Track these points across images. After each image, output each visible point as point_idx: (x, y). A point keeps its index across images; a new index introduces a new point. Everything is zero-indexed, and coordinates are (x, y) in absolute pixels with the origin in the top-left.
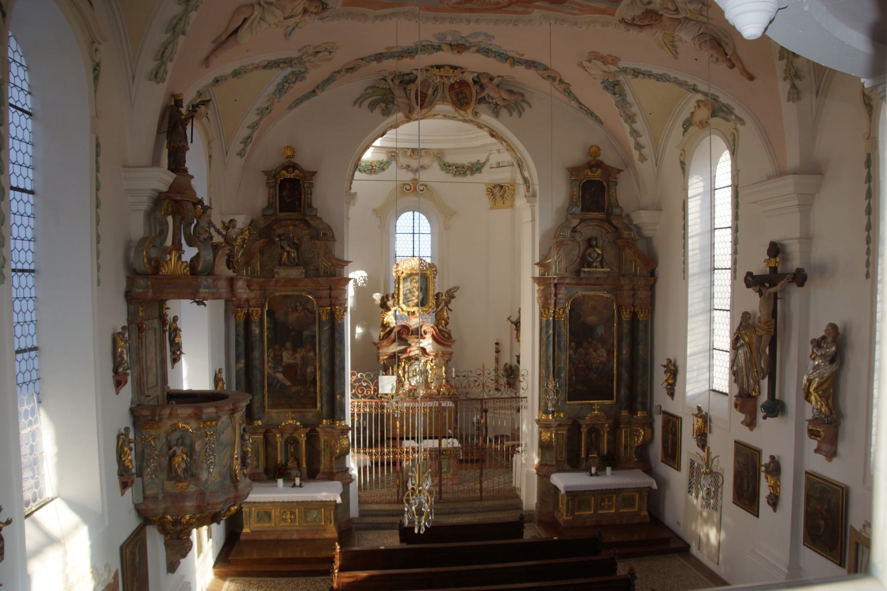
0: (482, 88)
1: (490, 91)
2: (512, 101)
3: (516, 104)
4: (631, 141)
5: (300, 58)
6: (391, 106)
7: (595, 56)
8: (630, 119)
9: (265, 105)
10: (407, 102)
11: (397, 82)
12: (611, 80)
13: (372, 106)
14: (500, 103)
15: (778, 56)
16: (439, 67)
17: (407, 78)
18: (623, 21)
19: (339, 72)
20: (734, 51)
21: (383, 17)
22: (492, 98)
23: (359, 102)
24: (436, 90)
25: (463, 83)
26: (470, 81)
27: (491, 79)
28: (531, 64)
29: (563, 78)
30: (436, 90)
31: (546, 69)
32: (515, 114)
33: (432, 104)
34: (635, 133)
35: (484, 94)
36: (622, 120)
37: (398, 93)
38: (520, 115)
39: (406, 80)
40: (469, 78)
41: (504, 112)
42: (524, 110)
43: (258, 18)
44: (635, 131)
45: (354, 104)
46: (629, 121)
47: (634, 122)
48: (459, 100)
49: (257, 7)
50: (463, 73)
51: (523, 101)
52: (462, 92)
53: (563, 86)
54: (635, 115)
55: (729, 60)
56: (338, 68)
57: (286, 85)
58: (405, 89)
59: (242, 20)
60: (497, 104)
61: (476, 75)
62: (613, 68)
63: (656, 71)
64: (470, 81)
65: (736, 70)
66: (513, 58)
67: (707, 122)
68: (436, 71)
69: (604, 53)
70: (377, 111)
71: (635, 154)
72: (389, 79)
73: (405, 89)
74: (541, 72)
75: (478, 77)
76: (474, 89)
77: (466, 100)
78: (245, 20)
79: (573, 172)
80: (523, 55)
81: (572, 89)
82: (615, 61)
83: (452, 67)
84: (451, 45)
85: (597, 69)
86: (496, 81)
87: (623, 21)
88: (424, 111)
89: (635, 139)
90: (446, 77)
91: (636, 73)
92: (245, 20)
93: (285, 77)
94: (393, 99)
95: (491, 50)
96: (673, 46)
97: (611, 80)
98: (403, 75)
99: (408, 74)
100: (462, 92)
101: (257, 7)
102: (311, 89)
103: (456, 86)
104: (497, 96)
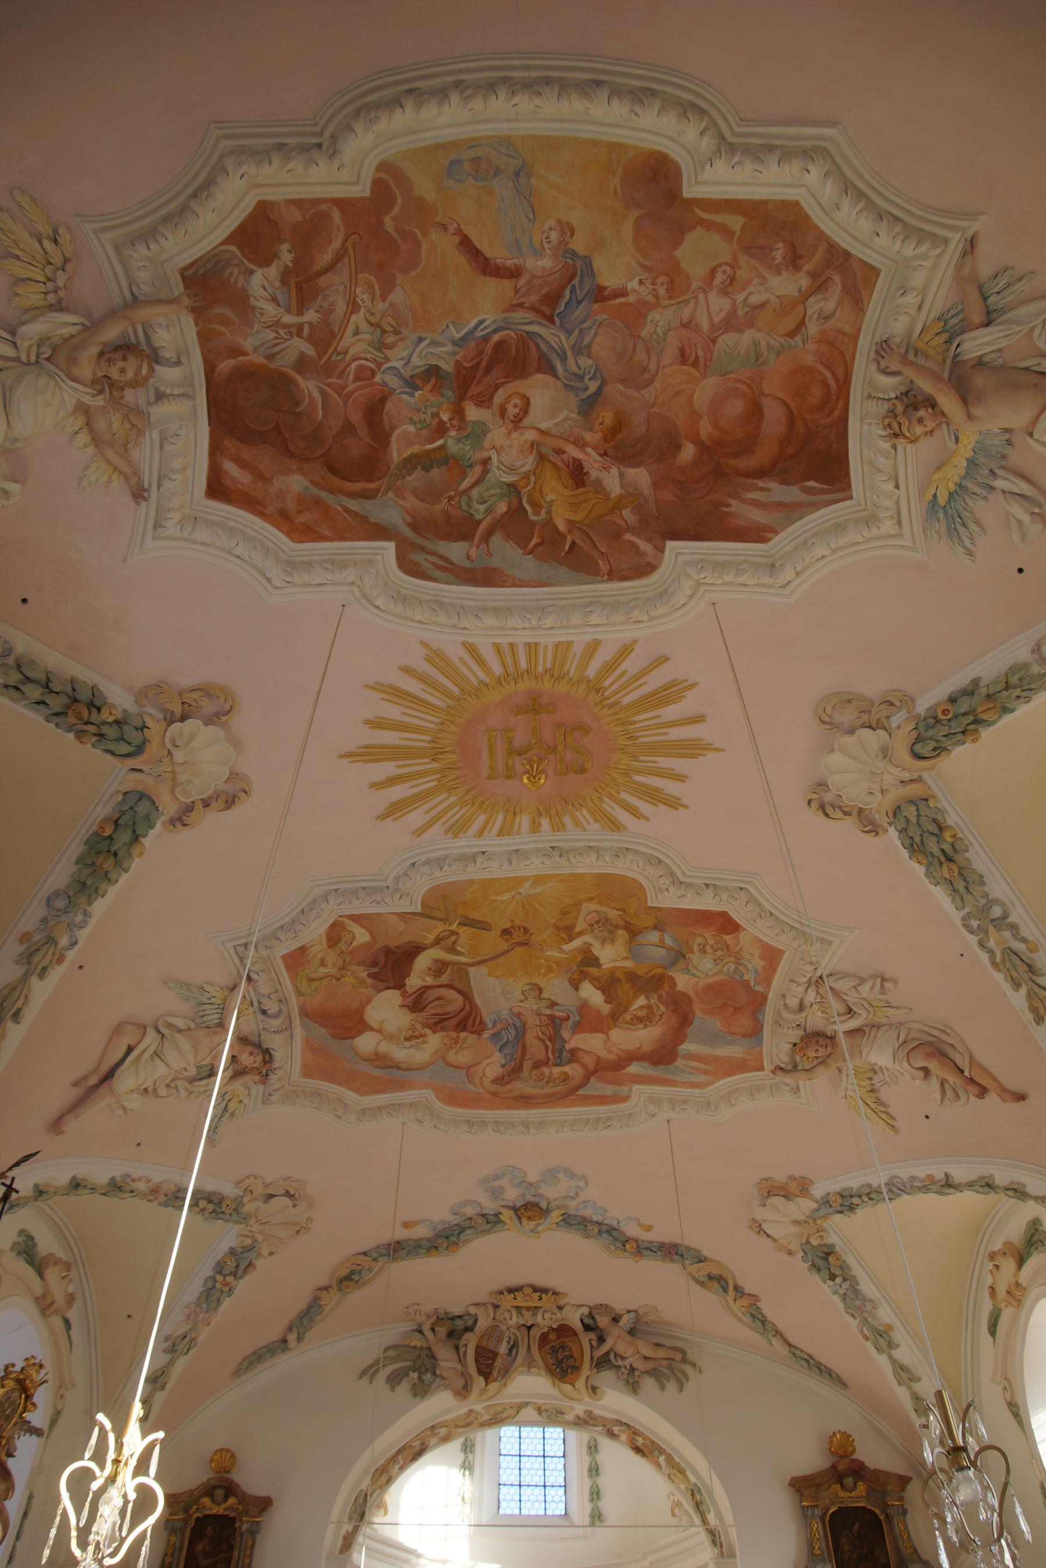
0: (601, 1340)
1: (616, 1341)
2: (660, 1359)
3: (670, 1367)
4: (902, 1394)
5: (239, 1203)
6: (428, 1377)
7: (773, 1190)
8: (883, 1338)
9: (181, 1331)
10: (459, 1367)
11: (442, 1331)
12: (815, 1242)
13: (394, 1380)
14: (640, 1365)
15: (1031, 1017)
16: (511, 1290)
17: (459, 1324)
18: (779, 1069)
19: (326, 1288)
20: (972, 1060)
21: (375, 1112)
22: (623, 1358)
23: (369, 1372)
24: (514, 1346)
25: (564, 1330)
26: (578, 1326)
27: (616, 1320)
28: (670, 1251)
29: (740, 1283)
30: (514, 1346)
31: (701, 1260)
32: (671, 1386)
33: (506, 1372)
34: (900, 1369)
35: (605, 1348)
36: (869, 1345)
37: (445, 1355)
38: (681, 1388)
39: (454, 1328)
40: (574, 1319)
41: (649, 1384)
42: (687, 1379)
43: (151, 1051)
44: (902, 1368)
45: (361, 1377)
46: (882, 1343)
47: (891, 1345)
48: (559, 1363)
49: (151, 1031)
50: (560, 1308)
51: (684, 1360)
52: (563, 1347)
53: (744, 1302)
54: (889, 1327)
55: (971, 1081)
56: (324, 1281)
57: (220, 1278)
58: (457, 1348)
59: (123, 1050)
60: (633, 1369)
61: (585, 1311)
62: (805, 1206)
63: (878, 1178)
64: (578, 1326)
65: (992, 1098)
66: (636, 1241)
67: (1018, 1285)
68: (508, 1301)
69: (780, 1176)
70: (404, 1387)
72: (426, 1328)
73: (457, 1348)
74: (693, 1269)
75: (591, 1315)
76: (586, 1339)
77: (571, 1362)
78: (130, 1049)
79: (803, 1487)
80: (649, 1228)
81: (767, 1307)
82: (802, 1187)
83: (535, 1289)
84: (515, 1209)
85: (783, 1219)
86: (626, 1321)
87: (779, 1069)
88: (493, 1386)
89: (910, 1388)
90: (528, 1309)
91: (847, 1202)
92: (130, 1049)
93: (218, 1263)
94: (434, 1366)
95: (591, 1221)
96: (879, 1101)
97: (815, 1242)
98: (452, 1319)
99: (460, 1317)
100: (563, 1347)
101: (151, 1031)
102: (274, 1333)
103: (553, 1336)
104: (630, 1352)
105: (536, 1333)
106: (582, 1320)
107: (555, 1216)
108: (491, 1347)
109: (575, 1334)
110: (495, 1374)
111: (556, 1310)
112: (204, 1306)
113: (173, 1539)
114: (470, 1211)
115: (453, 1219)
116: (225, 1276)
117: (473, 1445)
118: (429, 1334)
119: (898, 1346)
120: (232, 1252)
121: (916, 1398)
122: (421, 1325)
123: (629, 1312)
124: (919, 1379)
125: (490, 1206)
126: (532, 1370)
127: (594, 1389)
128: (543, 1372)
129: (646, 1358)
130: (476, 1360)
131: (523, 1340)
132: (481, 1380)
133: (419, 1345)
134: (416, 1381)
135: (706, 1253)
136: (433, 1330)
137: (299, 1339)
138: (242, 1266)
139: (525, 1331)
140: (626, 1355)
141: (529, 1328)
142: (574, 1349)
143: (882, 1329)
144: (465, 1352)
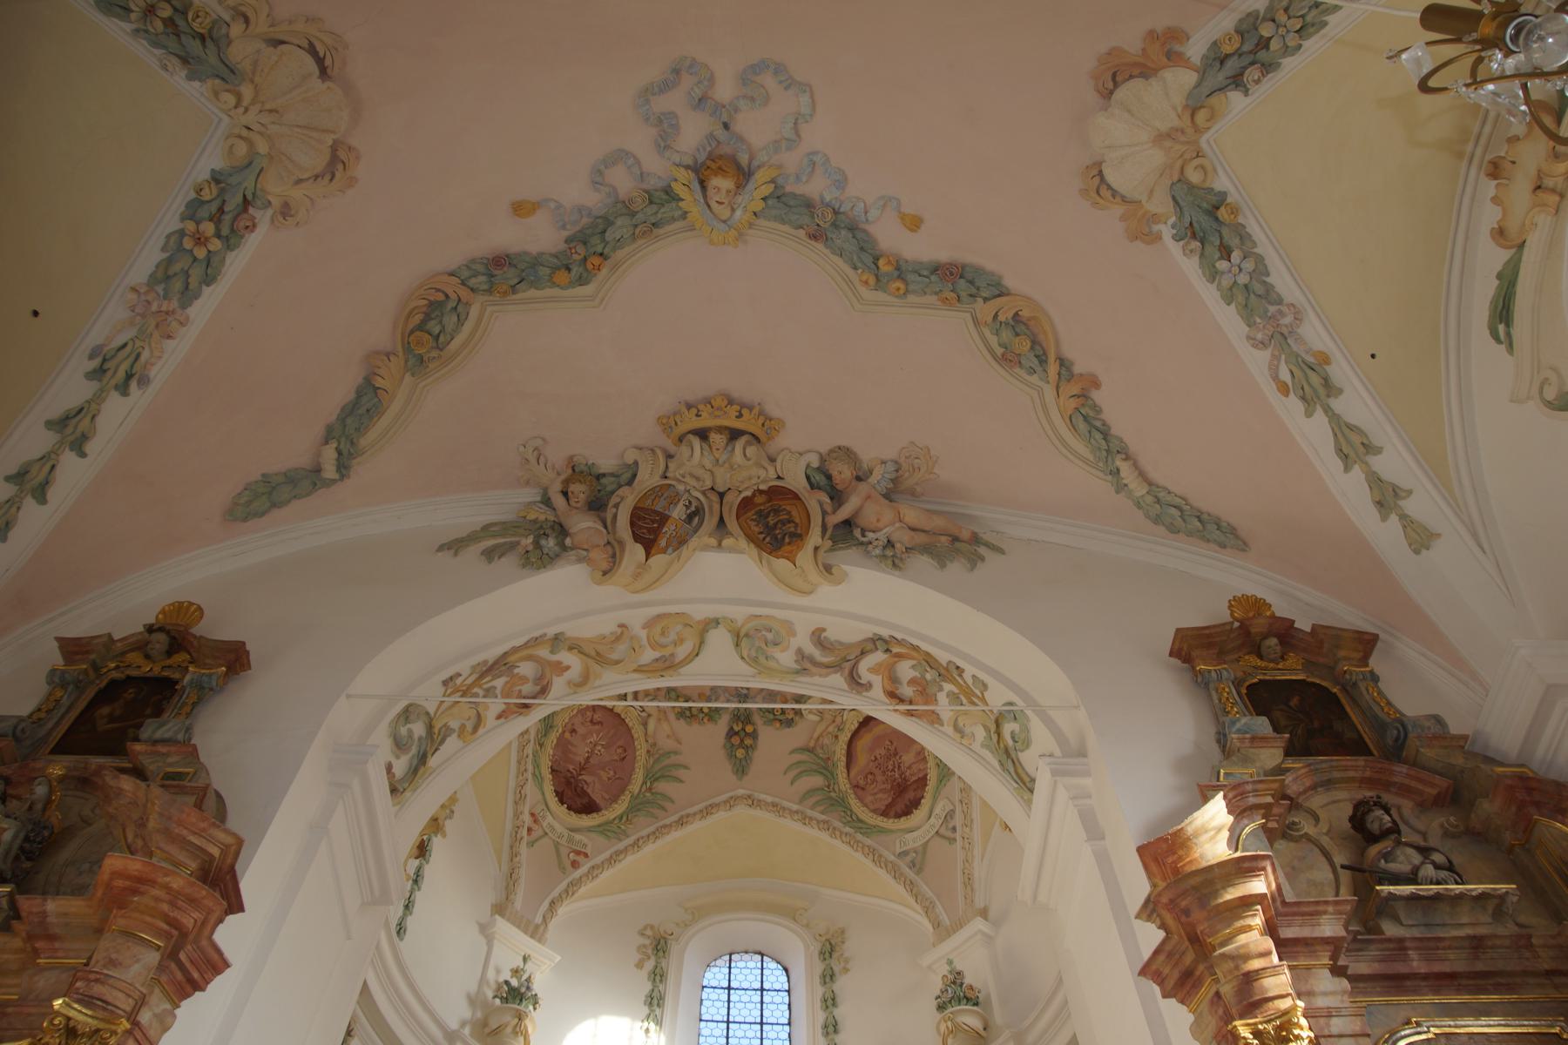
8: (1313, 383)
14: (903, 537)
25: (779, 494)
29: (1069, 352)
30: (695, 515)
33: (682, 542)
37: (583, 525)
40: (796, 480)
48: (769, 530)
52: (777, 511)
60: (890, 543)
70: (508, 563)
71: (1386, 536)
80: (914, 223)
86: (873, 479)
88: (658, 560)
105: (733, 500)
106: (808, 478)
107: (759, 187)
108: (659, 508)
109: (796, 497)
110: (663, 543)
111: (766, 463)
112: (160, 289)
113: (59, 694)
114: (622, 182)
115: (594, 200)
116: (198, 223)
117: (661, 999)
118: (559, 501)
119: (1340, 391)
120: (216, 178)
121: (1375, 481)
122: (545, 491)
123: (884, 462)
124: (1378, 451)
125: (657, 167)
126: (727, 542)
127: (828, 569)
128: (743, 543)
129: (913, 529)
130: (632, 524)
131: (711, 507)
132: (639, 550)
133: (542, 518)
134: (530, 548)
135: (1010, 282)
136: (565, 494)
137: (343, 468)
138: (233, 202)
139: (715, 498)
140: (880, 525)
141: (721, 495)
142: (794, 513)
143: (1310, 359)
144: (615, 516)
